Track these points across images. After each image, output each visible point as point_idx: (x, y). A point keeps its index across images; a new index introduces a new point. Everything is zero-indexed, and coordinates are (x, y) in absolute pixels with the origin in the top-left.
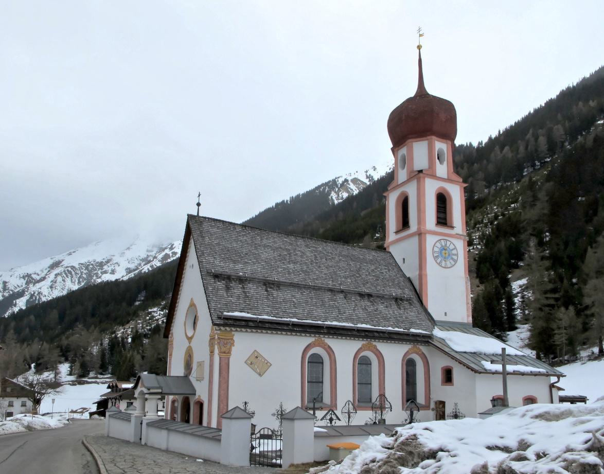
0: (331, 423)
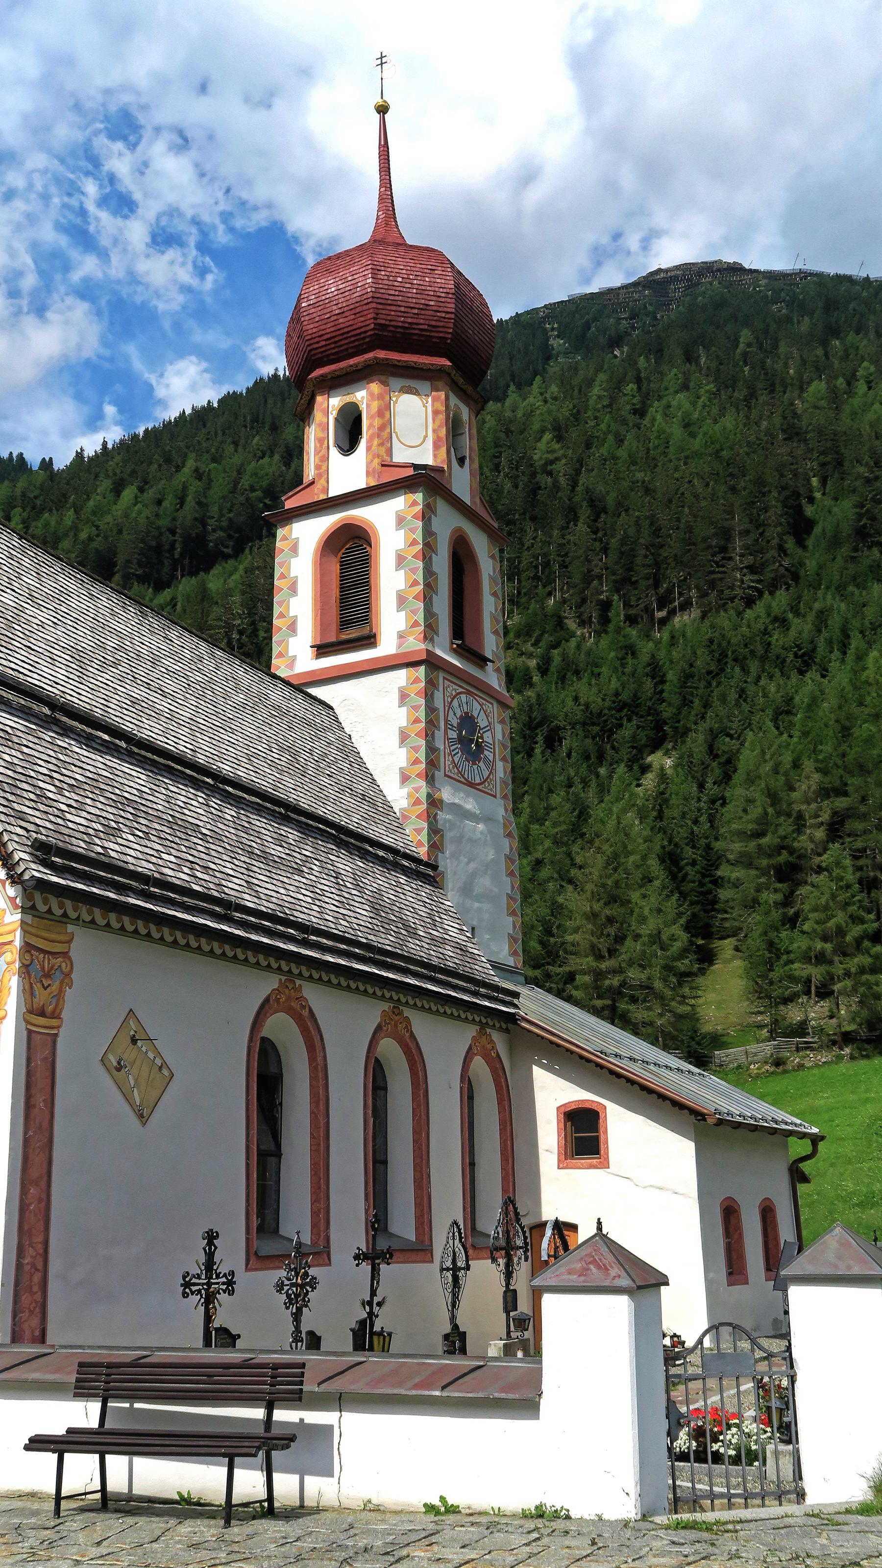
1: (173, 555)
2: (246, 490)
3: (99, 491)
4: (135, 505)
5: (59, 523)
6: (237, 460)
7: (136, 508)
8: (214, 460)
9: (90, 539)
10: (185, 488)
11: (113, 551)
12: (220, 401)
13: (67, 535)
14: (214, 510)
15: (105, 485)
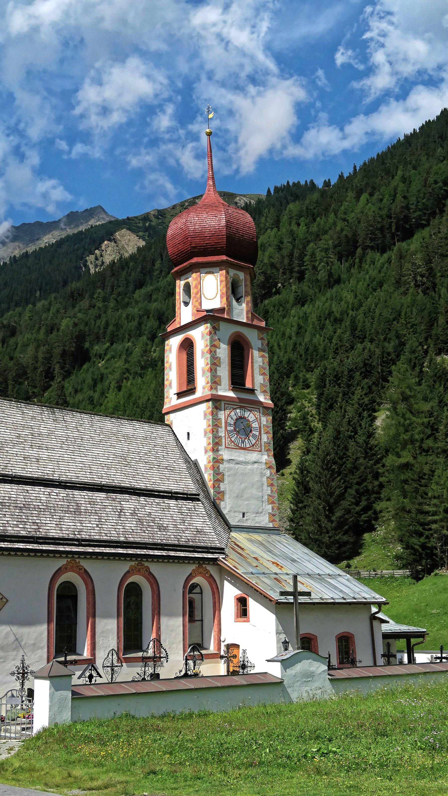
0: (90, 681)
1: (391, 231)
2: (432, 184)
3: (347, 199)
4: (367, 204)
5: (325, 223)
6: (427, 166)
7: (367, 207)
8: (415, 168)
9: (342, 230)
10: (395, 189)
11: (355, 234)
12: (420, 129)
13: (330, 229)
14: (413, 199)
15: (351, 195)
